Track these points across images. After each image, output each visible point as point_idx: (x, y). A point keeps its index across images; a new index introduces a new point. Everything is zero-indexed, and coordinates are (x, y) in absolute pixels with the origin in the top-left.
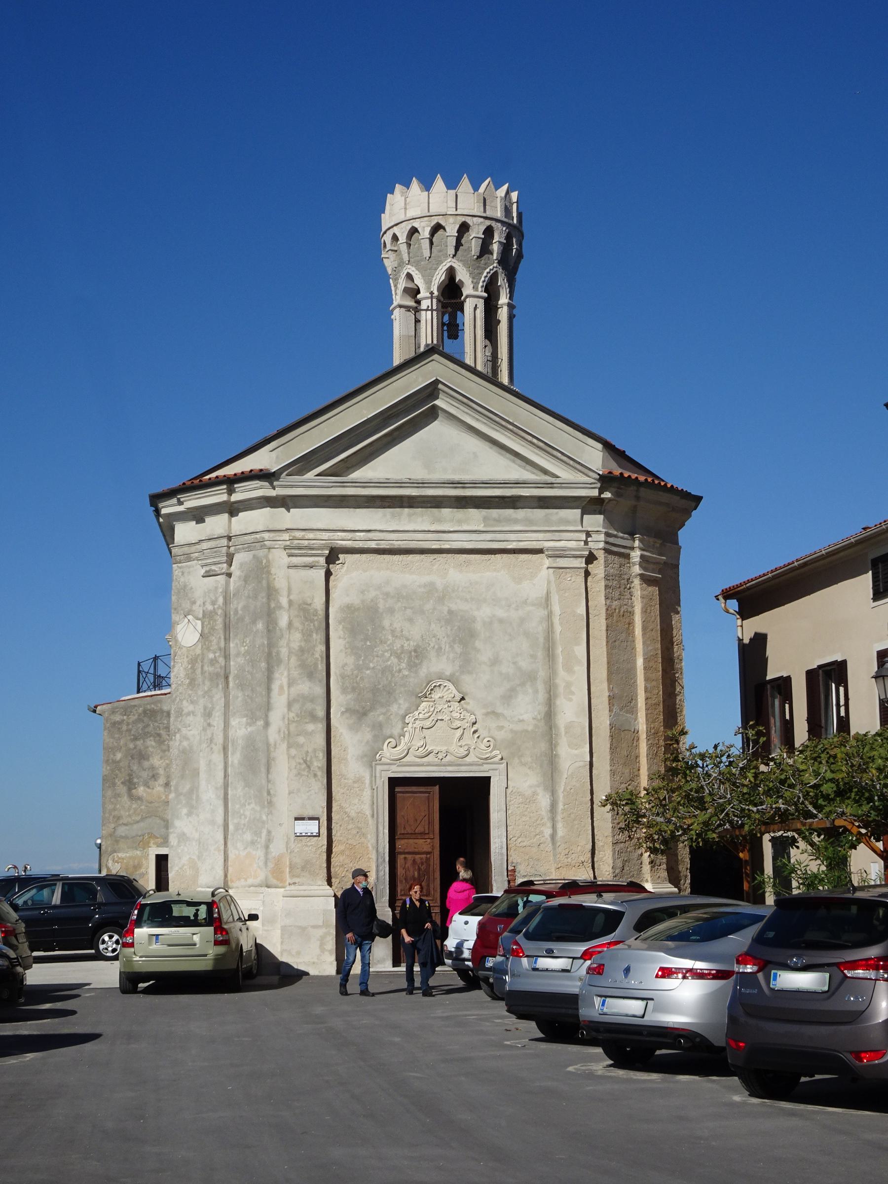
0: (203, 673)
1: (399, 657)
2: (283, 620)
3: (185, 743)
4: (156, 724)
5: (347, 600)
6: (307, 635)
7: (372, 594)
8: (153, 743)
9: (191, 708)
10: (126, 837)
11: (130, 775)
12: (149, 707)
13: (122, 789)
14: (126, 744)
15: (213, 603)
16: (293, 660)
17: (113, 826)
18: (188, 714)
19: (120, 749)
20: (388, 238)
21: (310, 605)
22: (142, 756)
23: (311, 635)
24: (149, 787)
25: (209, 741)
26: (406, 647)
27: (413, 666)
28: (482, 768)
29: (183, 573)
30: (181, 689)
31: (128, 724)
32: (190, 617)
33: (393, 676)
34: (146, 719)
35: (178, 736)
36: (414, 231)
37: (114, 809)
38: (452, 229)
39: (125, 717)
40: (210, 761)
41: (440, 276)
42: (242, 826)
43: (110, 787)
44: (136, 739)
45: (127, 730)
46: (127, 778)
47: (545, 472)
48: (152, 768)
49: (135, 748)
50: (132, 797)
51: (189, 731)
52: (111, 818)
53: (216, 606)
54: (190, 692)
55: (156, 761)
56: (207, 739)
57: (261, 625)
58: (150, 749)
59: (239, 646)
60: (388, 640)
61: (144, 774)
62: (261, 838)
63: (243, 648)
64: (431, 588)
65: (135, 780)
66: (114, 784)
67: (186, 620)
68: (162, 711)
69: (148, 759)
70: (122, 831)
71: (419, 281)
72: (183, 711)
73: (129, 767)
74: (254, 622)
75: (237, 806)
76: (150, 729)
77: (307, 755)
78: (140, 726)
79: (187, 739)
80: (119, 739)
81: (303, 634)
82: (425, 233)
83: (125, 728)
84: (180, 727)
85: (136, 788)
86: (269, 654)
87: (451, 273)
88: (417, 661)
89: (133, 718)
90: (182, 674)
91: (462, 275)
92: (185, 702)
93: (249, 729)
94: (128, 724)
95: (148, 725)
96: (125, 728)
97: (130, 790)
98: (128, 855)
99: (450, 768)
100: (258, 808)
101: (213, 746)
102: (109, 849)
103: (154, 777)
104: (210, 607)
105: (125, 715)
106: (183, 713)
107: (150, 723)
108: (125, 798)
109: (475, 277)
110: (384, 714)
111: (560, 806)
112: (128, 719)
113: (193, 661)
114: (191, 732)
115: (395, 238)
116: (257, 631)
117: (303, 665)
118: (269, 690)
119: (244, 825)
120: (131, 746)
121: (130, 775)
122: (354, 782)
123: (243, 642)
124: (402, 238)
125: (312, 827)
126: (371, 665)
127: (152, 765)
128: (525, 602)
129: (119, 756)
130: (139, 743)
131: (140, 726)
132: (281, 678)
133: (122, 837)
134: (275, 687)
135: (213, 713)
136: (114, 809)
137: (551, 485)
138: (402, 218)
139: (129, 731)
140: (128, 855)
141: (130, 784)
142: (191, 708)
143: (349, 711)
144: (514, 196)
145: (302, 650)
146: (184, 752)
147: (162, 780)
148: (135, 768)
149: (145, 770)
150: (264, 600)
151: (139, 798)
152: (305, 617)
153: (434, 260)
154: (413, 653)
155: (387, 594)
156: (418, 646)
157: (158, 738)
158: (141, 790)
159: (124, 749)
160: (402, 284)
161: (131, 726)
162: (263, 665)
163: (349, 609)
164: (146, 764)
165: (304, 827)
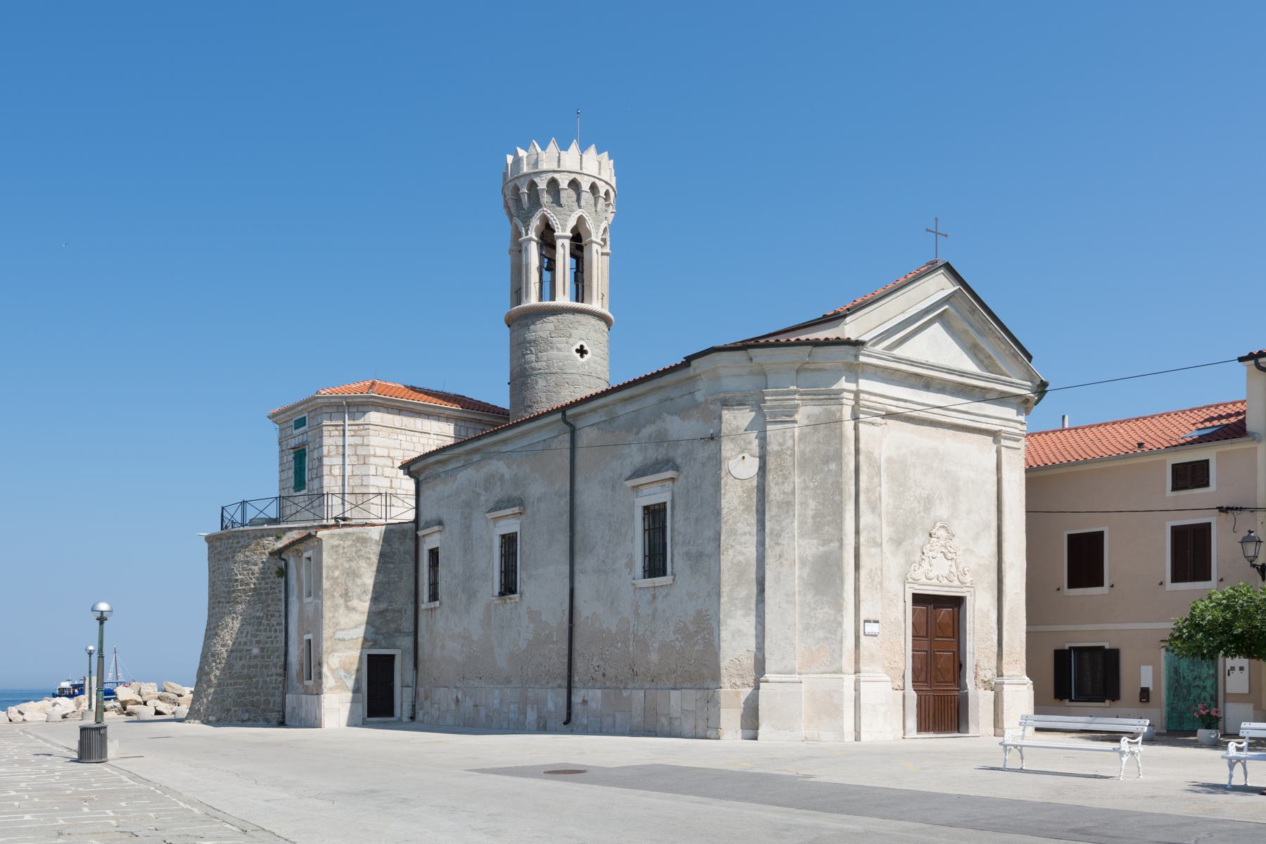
3: (741, 558)
4: (367, 550)
8: (365, 565)
10: (343, 640)
11: (346, 590)
12: (361, 535)
13: (341, 601)
14: (342, 565)
15: (781, 445)
17: (332, 630)
19: (337, 568)
21: (872, 454)
23: (873, 478)
24: (361, 600)
25: (778, 557)
26: (923, 495)
27: (927, 509)
28: (962, 590)
29: (735, 417)
30: (734, 513)
31: (344, 548)
32: (746, 455)
33: (915, 516)
34: (358, 545)
35: (731, 552)
37: (334, 617)
39: (342, 542)
40: (779, 573)
42: (813, 626)
43: (329, 598)
45: (343, 553)
46: (344, 592)
49: (350, 568)
50: (347, 607)
51: (745, 547)
52: (330, 624)
53: (784, 447)
54: (747, 516)
56: (775, 555)
57: (834, 466)
58: (363, 569)
59: (807, 482)
60: (912, 487)
62: (836, 635)
63: (812, 484)
65: (350, 594)
66: (333, 596)
67: (741, 456)
68: (371, 539)
69: (359, 576)
70: (340, 635)
72: (737, 531)
73: (346, 583)
75: (807, 610)
76: (362, 553)
77: (871, 572)
78: (354, 549)
80: (337, 559)
81: (869, 477)
84: (733, 544)
85: (350, 601)
88: (929, 506)
89: (349, 543)
90: (736, 501)
93: (821, 549)
94: (344, 548)
95: (360, 550)
96: (341, 551)
97: (346, 601)
98: (345, 654)
99: (946, 589)
100: (832, 612)
101: (783, 560)
102: (330, 649)
105: (341, 540)
106: (738, 533)
107: (362, 548)
108: (342, 610)
110: (911, 545)
112: (345, 544)
114: (747, 549)
116: (830, 470)
119: (815, 625)
120: (347, 566)
121: (346, 590)
122: (894, 595)
123: (813, 479)
126: (903, 506)
127: (364, 582)
129: (337, 573)
130: (354, 564)
131: (354, 549)
133: (339, 640)
135: (783, 534)
136: (334, 617)
139: (344, 553)
140: (345, 654)
143: (891, 539)
146: (739, 563)
148: (350, 585)
149: (358, 586)
151: (354, 609)
152: (870, 464)
154: (927, 500)
156: (929, 495)
157: (368, 561)
159: (340, 568)
161: (346, 550)
164: (359, 582)
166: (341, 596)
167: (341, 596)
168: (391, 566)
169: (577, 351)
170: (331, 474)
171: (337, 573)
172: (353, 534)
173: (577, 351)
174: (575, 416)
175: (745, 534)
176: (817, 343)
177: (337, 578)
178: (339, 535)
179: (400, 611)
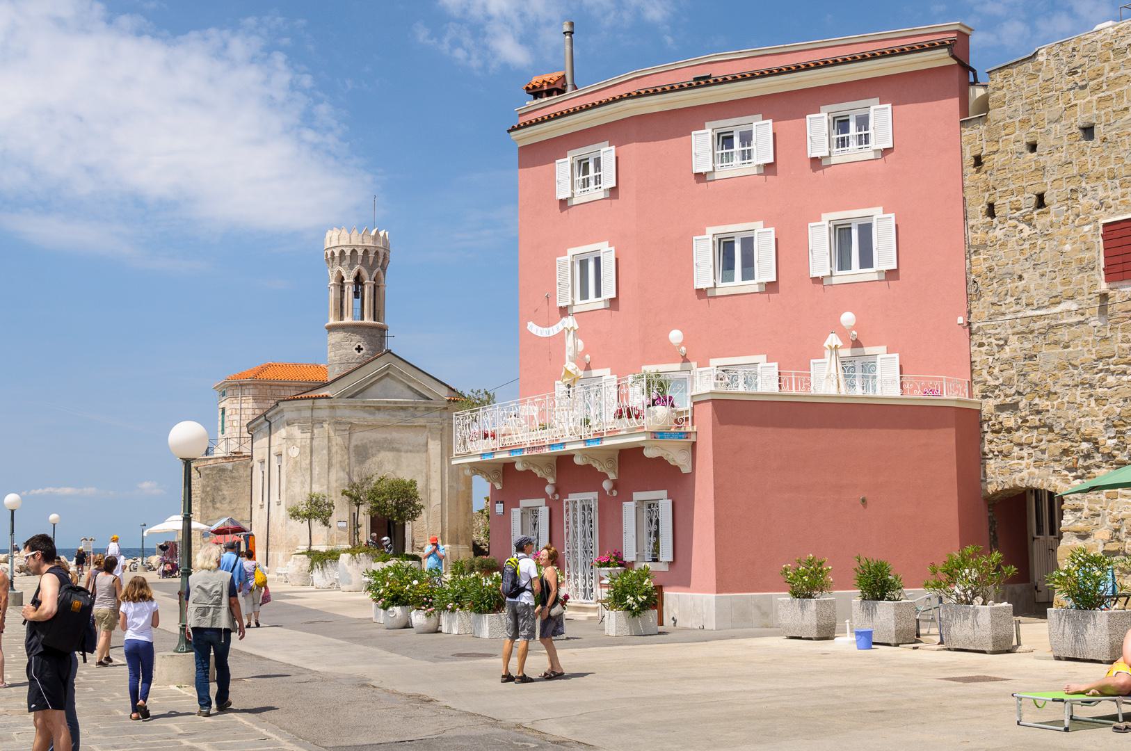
0: (301, 468)
1: (375, 464)
2: (334, 450)
3: (292, 493)
5: (356, 443)
6: (342, 456)
7: (365, 441)
9: (295, 480)
13: (211, 504)
16: (338, 465)
18: (294, 482)
19: (208, 486)
20: (329, 252)
22: (217, 489)
36: (342, 252)
38: (360, 253)
41: (354, 273)
44: (216, 482)
47: (428, 398)
48: (223, 495)
50: (214, 507)
55: (225, 493)
61: (220, 498)
64: (386, 440)
68: (227, 469)
71: (344, 274)
74: (322, 450)
78: (218, 475)
79: (293, 491)
82: (348, 253)
83: (211, 477)
86: (329, 462)
87: (359, 273)
89: (215, 472)
91: (365, 273)
92: (292, 478)
96: (211, 477)
103: (224, 499)
104: (303, 444)
109: (370, 275)
111: (430, 517)
113: (296, 462)
115: (333, 254)
117: (341, 466)
118: (328, 475)
120: (214, 485)
124: (337, 254)
125: (344, 524)
128: (419, 445)
129: (208, 489)
132: (333, 471)
134: (331, 474)
137: (430, 403)
138: (337, 245)
141: (213, 501)
142: (295, 480)
144: (387, 233)
145: (341, 462)
147: (228, 501)
148: (215, 495)
150: (327, 443)
153: (351, 266)
155: (370, 441)
158: (218, 505)
160: (335, 275)
162: (326, 466)
163: (356, 446)
164: (220, 493)
165: (341, 524)
166: (210, 501)
167: (210, 501)
168: (239, 484)
169: (356, 349)
170: (232, 426)
171: (208, 489)
172: (217, 467)
173: (356, 349)
174: (270, 417)
175: (294, 482)
176: (316, 398)
177: (208, 492)
178: (210, 468)
179: (243, 509)
